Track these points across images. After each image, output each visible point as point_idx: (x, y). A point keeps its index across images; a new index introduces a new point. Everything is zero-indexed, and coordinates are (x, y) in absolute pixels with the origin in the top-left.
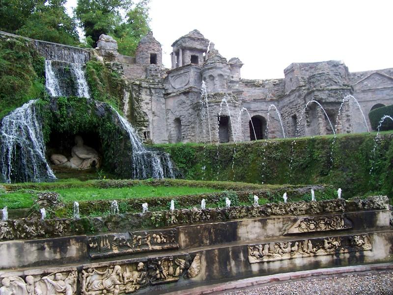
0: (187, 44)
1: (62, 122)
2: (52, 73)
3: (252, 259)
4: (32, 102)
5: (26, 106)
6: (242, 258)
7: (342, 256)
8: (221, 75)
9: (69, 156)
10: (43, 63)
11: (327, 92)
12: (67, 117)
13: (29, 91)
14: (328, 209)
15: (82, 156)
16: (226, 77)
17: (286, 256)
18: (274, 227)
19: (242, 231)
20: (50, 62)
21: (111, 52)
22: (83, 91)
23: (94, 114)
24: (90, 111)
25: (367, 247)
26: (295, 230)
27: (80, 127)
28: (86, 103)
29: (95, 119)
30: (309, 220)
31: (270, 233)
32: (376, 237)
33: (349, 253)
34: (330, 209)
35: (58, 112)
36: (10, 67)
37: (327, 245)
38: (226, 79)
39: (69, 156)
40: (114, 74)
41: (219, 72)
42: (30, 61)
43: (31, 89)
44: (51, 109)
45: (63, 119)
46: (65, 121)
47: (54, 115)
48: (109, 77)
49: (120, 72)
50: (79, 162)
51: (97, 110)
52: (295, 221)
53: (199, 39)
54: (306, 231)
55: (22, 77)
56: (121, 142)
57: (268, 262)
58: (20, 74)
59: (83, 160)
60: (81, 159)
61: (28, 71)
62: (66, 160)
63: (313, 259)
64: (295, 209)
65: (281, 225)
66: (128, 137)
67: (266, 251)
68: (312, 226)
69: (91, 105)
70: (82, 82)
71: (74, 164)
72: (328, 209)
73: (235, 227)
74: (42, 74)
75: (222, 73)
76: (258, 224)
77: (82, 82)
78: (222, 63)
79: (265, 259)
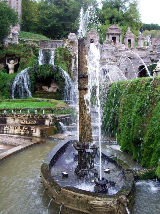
0: (109, 32)
1: (38, 75)
2: (42, 54)
3: (4, 129)
4: (29, 67)
5: (26, 69)
6: (2, 128)
7: (27, 133)
8: (107, 50)
9: (49, 86)
10: (38, 51)
11: (156, 55)
12: (40, 72)
13: (29, 63)
14: (34, 117)
15: (53, 87)
16: (110, 50)
17: (13, 130)
18: (17, 121)
19: (8, 121)
20: (42, 49)
21: (72, 40)
22: (52, 62)
23: (51, 71)
24: (50, 70)
25: (34, 131)
26: (22, 123)
27: (46, 76)
28: (49, 66)
29: (51, 73)
30: (26, 120)
31: (16, 122)
32: (37, 128)
33: (29, 132)
34: (35, 117)
35: (37, 71)
36: (23, 55)
37: (23, 128)
38: (110, 51)
39: (49, 86)
40: (67, 51)
41: (106, 48)
42: (32, 51)
43: (30, 62)
44: (34, 70)
45: (38, 74)
46: (39, 74)
47: (36, 73)
48: (65, 53)
49: (70, 51)
50: (53, 89)
51: (53, 69)
52: (23, 119)
53: (115, 29)
54: (25, 123)
55: (27, 57)
56: (62, 82)
57: (8, 131)
58: (27, 57)
59: (54, 88)
60: (53, 88)
61: (30, 55)
62: (48, 88)
63: (19, 132)
64: (26, 116)
65: (19, 121)
66: (64, 80)
67: (8, 127)
68: (27, 122)
69: (50, 67)
70: (52, 57)
71: (50, 90)
72: (34, 117)
73: (6, 119)
74: (37, 55)
75: (107, 49)
76: (13, 119)
77: (52, 57)
78: (108, 44)
79: (8, 130)
